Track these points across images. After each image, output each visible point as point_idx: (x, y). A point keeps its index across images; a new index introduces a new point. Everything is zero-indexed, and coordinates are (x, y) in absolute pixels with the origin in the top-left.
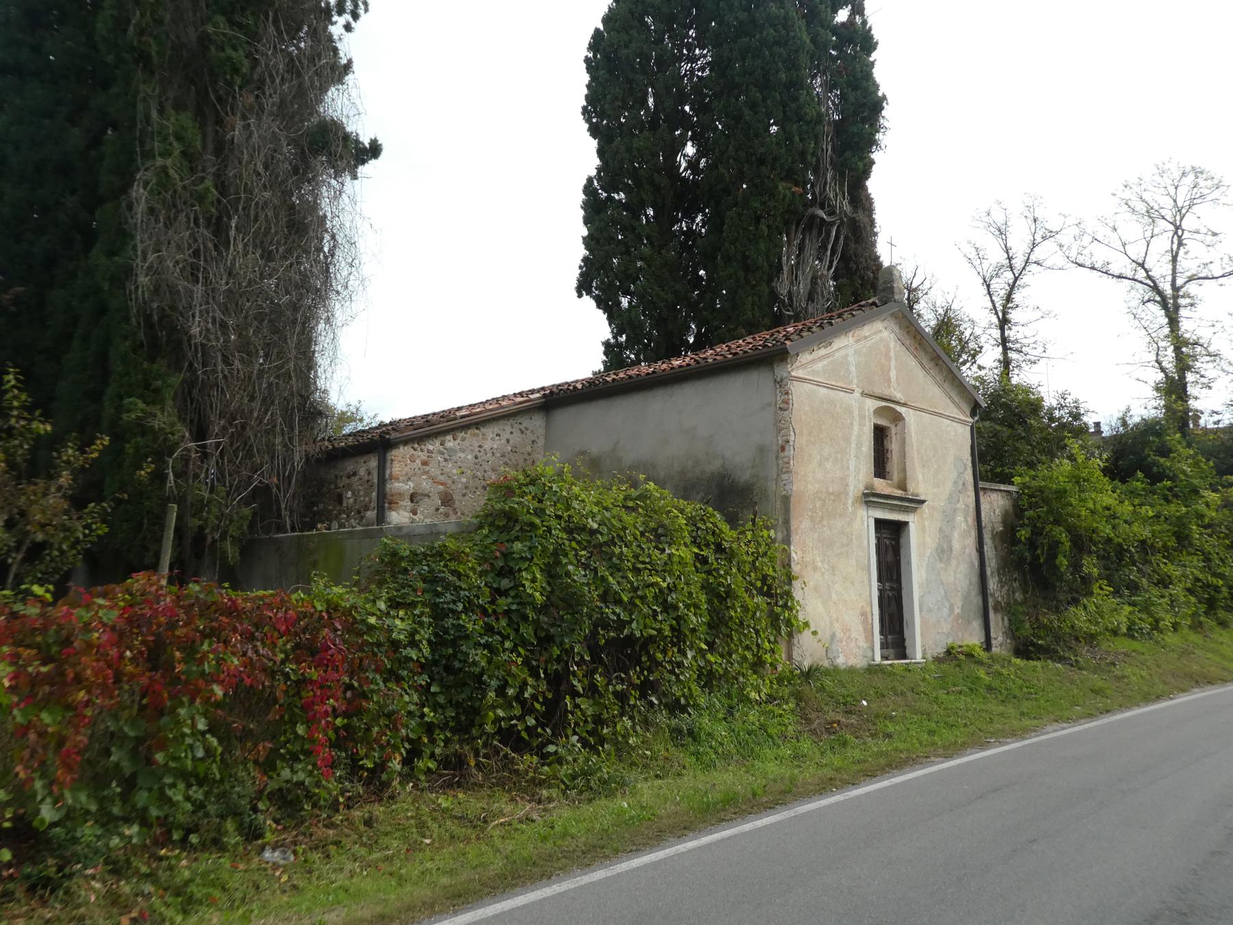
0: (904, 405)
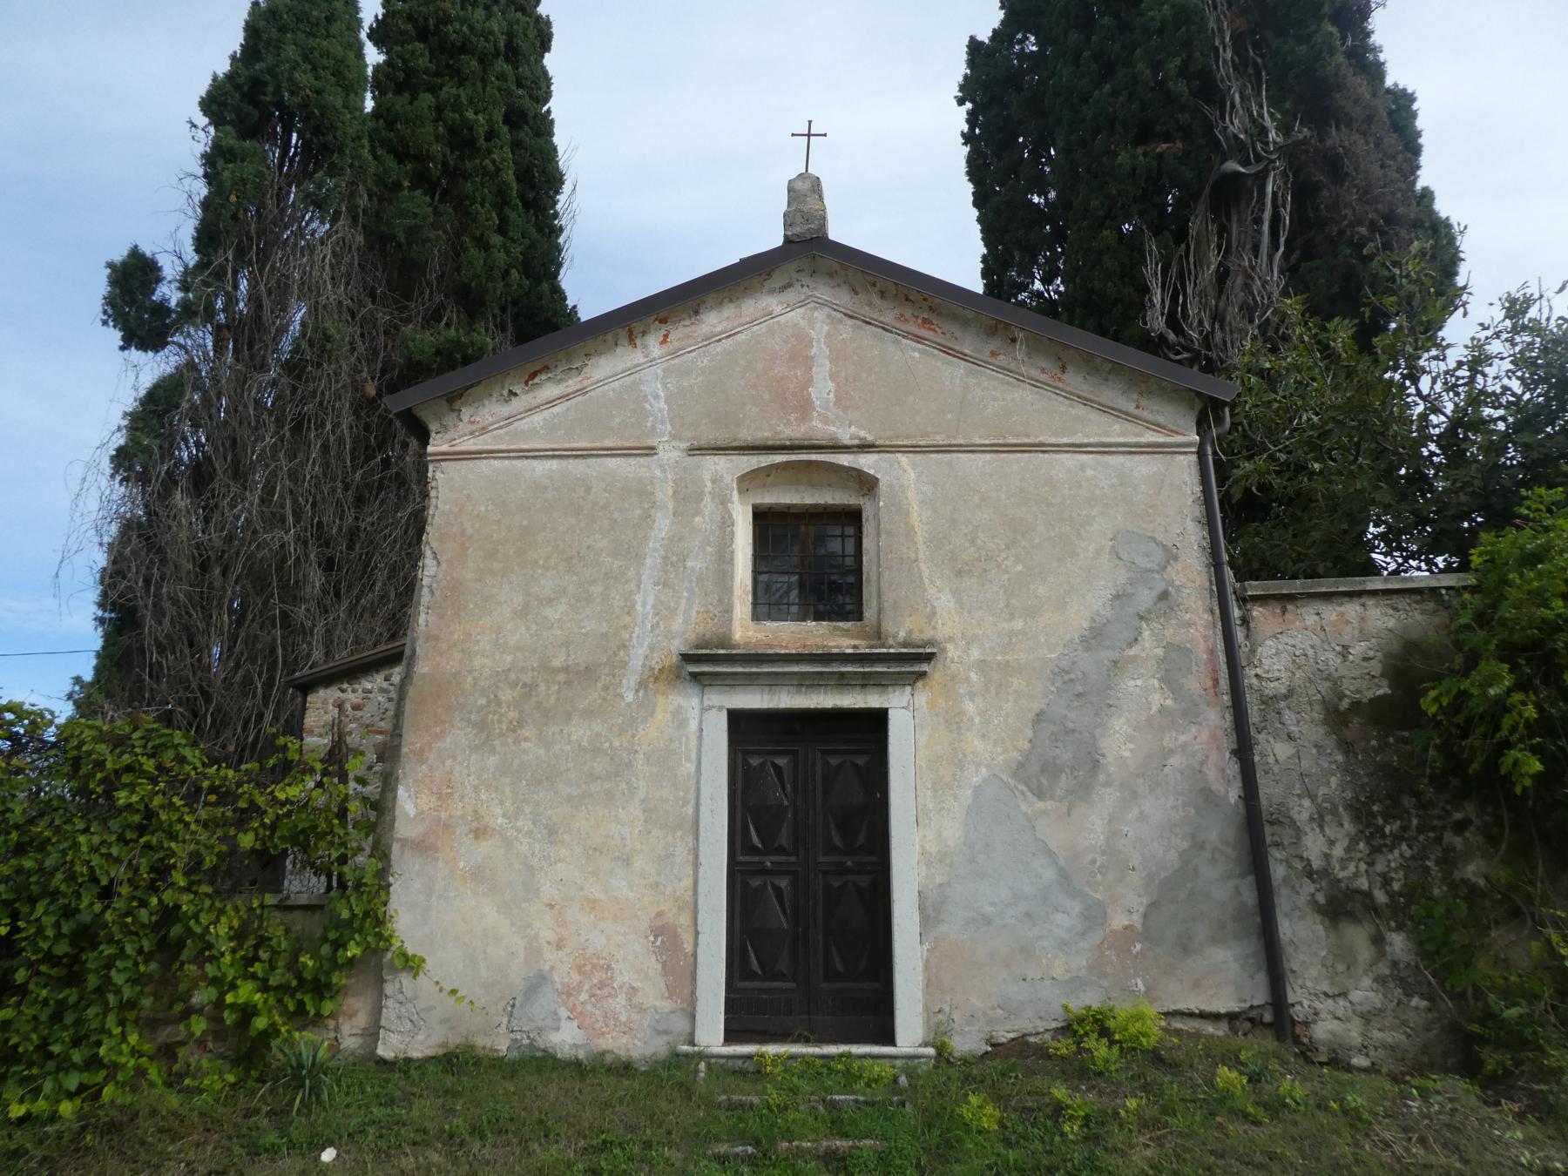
0: (865, 447)
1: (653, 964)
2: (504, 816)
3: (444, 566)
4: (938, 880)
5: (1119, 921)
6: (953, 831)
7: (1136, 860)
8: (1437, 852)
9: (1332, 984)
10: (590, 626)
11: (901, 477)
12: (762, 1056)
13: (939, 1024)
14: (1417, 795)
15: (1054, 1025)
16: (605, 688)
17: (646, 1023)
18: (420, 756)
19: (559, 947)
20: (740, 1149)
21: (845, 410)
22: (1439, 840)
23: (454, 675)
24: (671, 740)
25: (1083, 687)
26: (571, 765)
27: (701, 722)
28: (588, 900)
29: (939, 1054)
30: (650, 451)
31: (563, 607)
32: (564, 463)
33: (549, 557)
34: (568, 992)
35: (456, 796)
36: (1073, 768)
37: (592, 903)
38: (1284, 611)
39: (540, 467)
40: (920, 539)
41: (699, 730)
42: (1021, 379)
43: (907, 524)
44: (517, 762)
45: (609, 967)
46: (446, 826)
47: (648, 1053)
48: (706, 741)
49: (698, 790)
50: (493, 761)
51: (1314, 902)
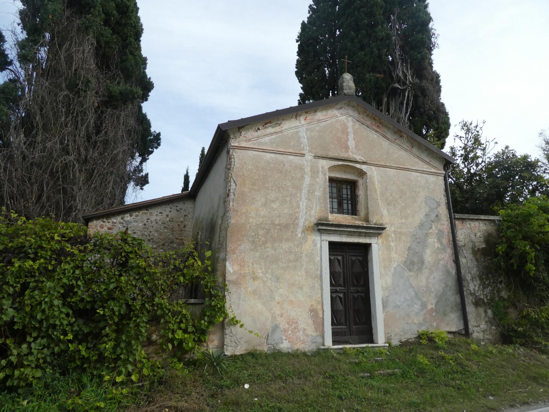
0: (364, 163)
1: (310, 321)
2: (262, 273)
3: (238, 186)
4: (386, 295)
5: (430, 307)
6: (389, 280)
7: (433, 290)
8: (496, 289)
9: (477, 323)
10: (286, 211)
11: (372, 172)
12: (346, 348)
13: (389, 337)
14: (492, 274)
15: (415, 336)
16: (292, 232)
17: (309, 340)
18: (233, 252)
19: (282, 317)
20: (366, 375)
21: (358, 150)
22: (497, 286)
23: (243, 224)
24: (312, 250)
25: (420, 240)
26: (283, 257)
27: (321, 245)
28: (290, 301)
29: (390, 345)
30: (303, 155)
31: (277, 204)
32: (276, 155)
33: (272, 187)
34: (285, 331)
35: (246, 266)
36: (418, 263)
37: (291, 302)
38: (463, 222)
39: (269, 156)
40: (378, 193)
41: (319, 247)
42: (403, 148)
43: (375, 188)
44: (265, 255)
45: (297, 323)
46: (244, 276)
47: (310, 349)
48: (323, 251)
49: (321, 266)
50: (258, 254)
51: (472, 302)
